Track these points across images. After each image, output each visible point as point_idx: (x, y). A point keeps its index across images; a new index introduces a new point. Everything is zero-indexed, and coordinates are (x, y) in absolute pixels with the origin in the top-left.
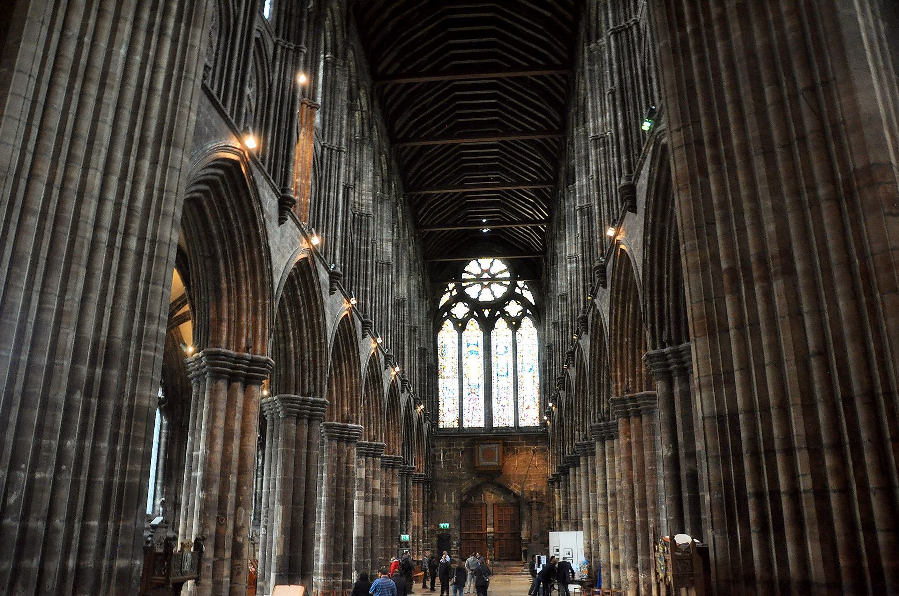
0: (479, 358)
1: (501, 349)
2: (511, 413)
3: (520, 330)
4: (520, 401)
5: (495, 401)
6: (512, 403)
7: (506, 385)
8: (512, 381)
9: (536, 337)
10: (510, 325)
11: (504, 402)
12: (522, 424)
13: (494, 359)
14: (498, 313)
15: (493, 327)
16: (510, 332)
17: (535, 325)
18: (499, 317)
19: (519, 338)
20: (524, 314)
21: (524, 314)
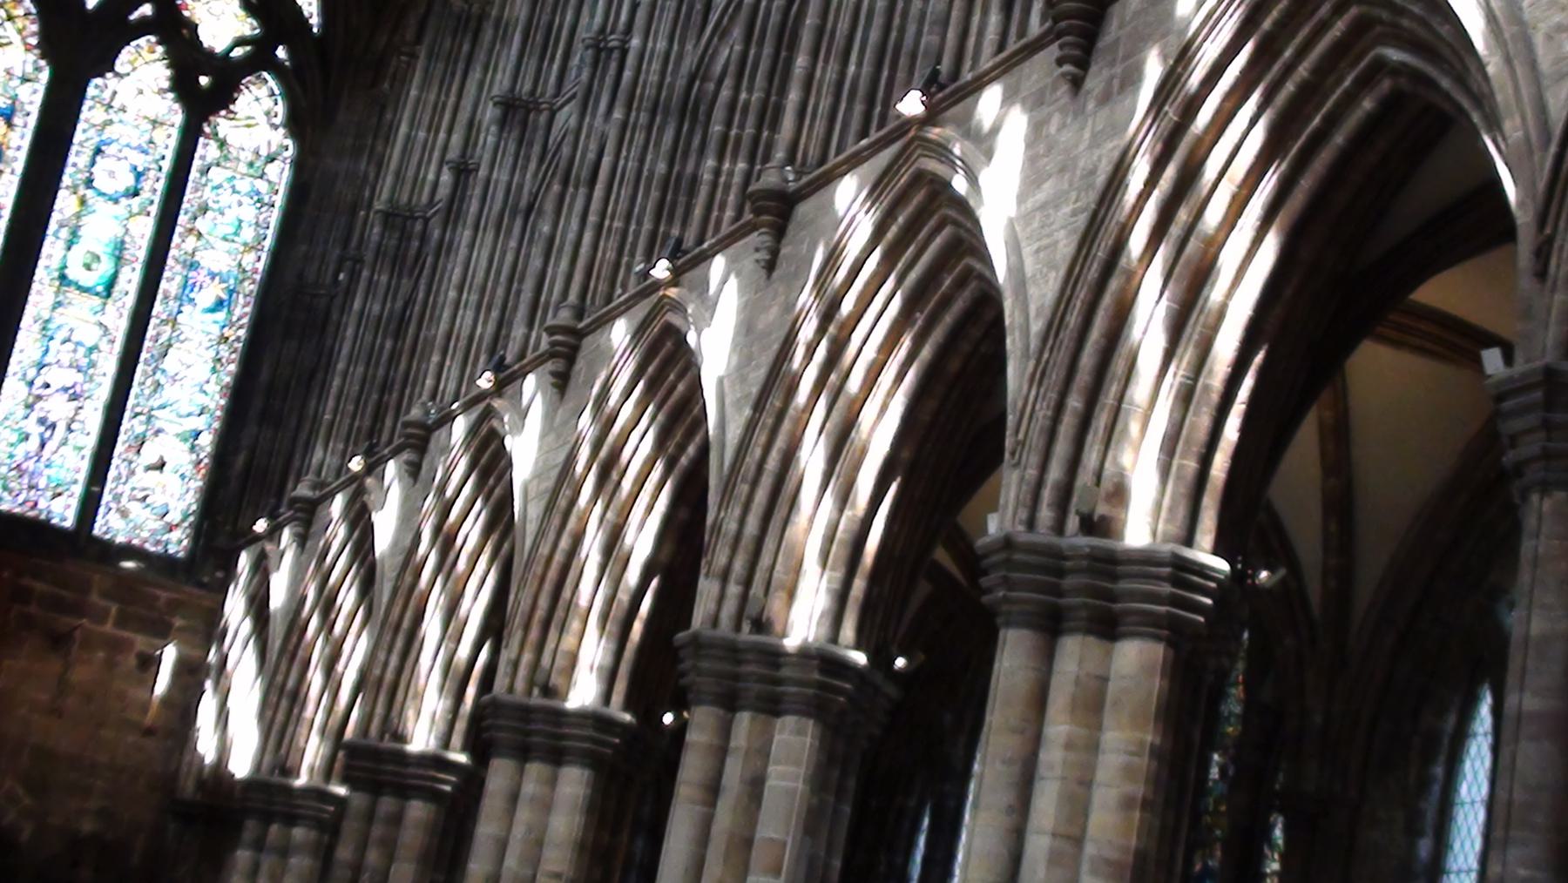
1: (113, 175)
2: (73, 464)
3: (223, 125)
4: (130, 426)
6: (93, 418)
7: (91, 336)
8: (120, 325)
9: (280, 174)
10: (182, 86)
11: (57, 408)
12: (110, 525)
13: (65, 204)
14: (146, 10)
15: (105, 65)
16: (174, 114)
17: (296, 124)
18: (143, 27)
19: (206, 151)
20: (259, 58)
21: (259, 58)
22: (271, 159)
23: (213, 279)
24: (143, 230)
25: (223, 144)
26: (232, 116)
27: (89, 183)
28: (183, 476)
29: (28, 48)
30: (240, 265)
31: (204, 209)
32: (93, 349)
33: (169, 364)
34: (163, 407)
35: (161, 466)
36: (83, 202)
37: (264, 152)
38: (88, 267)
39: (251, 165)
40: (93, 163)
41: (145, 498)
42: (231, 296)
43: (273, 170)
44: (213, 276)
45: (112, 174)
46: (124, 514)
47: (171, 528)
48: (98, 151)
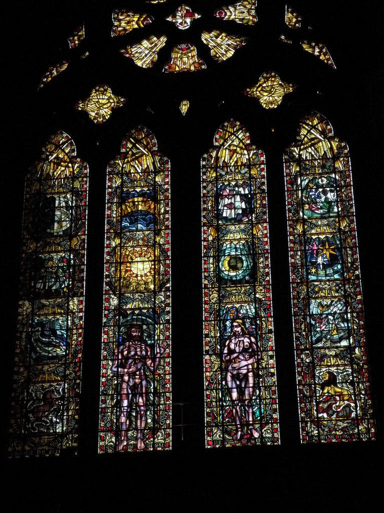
0: (157, 233)
5: (211, 363)
7: (250, 310)
22: (335, 158)
23: (324, 245)
24: (262, 231)
25: (299, 161)
26: (299, 143)
27: (219, 216)
28: (352, 383)
29: (153, 154)
30: (340, 229)
31: (301, 204)
32: (257, 316)
33: (314, 309)
34: (319, 340)
35: (332, 381)
36: (218, 229)
37: (329, 155)
38: (233, 268)
39: (323, 167)
40: (217, 204)
41: (330, 407)
42: (341, 252)
43: (339, 165)
44: (322, 243)
45: (231, 206)
46: (318, 423)
47: (356, 422)
48: (218, 196)
